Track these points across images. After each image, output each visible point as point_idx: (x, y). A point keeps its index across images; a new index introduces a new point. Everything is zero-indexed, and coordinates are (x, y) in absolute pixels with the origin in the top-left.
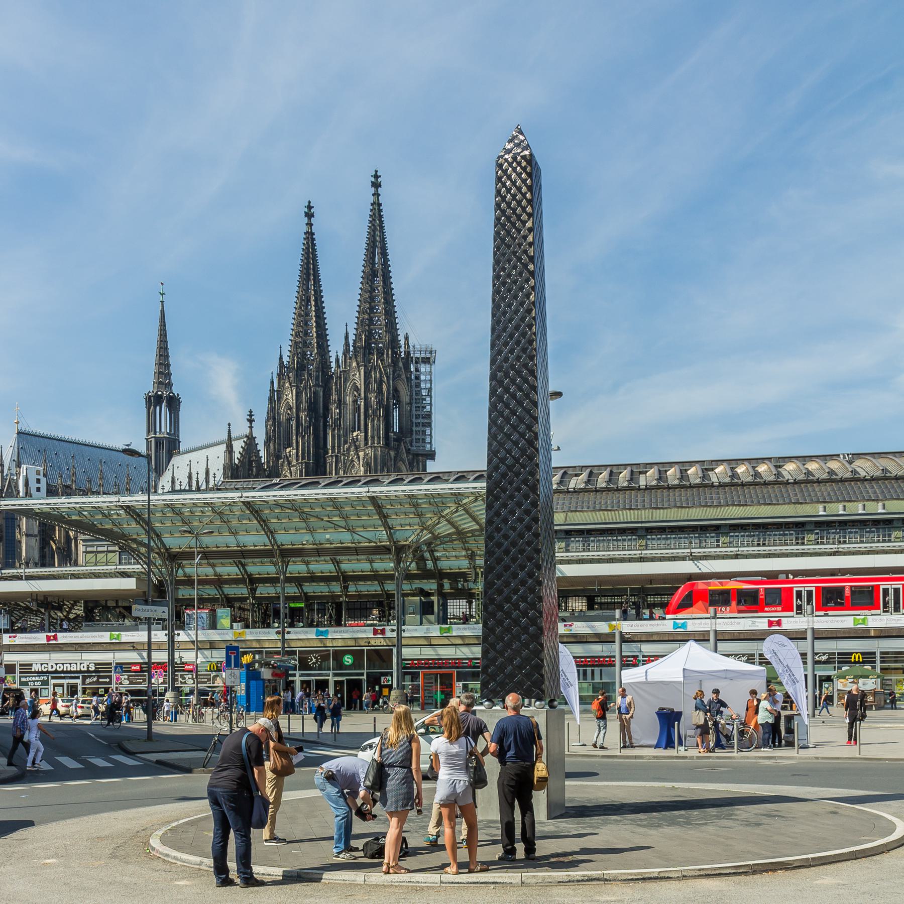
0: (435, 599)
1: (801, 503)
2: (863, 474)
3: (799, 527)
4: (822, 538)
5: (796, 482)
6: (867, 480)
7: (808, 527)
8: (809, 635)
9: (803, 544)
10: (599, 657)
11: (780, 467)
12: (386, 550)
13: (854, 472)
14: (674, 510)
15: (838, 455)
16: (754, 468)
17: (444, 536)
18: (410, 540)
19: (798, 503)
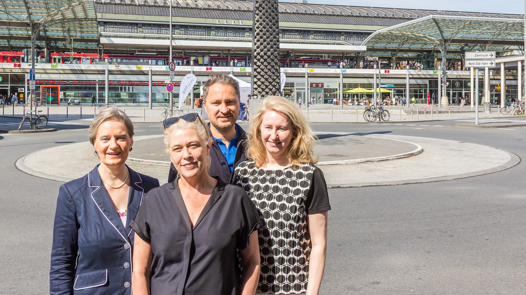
0: (45, 50)
2: (200, 6)
3: (208, 28)
4: (218, 33)
7: (212, 29)
8: (150, 73)
10: (39, 80)
12: (28, 25)
14: (153, 17)
17: (56, 20)
18: (40, 20)
19: (206, 18)
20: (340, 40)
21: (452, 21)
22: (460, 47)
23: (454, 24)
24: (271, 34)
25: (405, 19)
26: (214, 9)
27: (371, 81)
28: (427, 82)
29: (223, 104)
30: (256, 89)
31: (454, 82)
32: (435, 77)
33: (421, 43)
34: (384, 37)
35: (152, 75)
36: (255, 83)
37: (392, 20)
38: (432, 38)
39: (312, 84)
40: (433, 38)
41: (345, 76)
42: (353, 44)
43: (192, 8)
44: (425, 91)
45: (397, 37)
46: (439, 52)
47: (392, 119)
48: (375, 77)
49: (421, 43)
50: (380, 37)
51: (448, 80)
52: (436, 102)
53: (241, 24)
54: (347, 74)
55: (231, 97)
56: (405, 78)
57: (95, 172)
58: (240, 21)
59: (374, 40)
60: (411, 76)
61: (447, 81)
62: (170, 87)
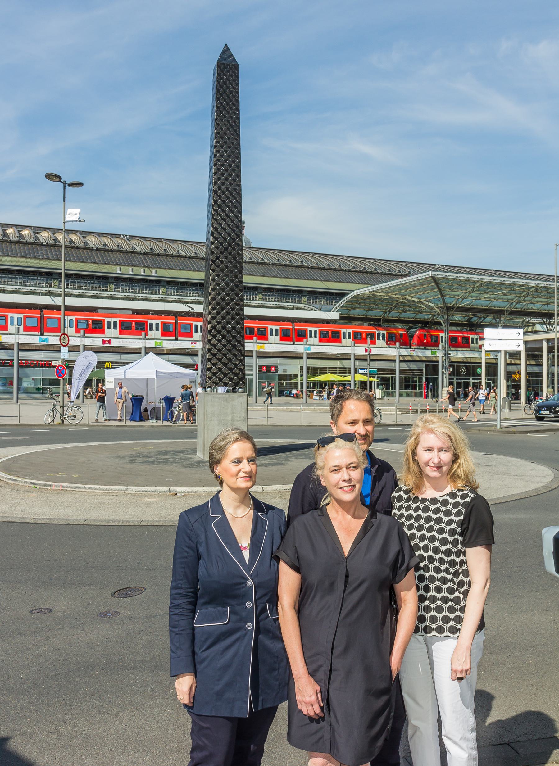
1: (102, 264)
3: (103, 280)
4: (119, 288)
5: (48, 245)
6: (141, 254)
7: (110, 280)
9: (107, 290)
11: (38, 233)
13: (86, 243)
15: (120, 235)
16: (19, 231)
19: (100, 263)
20: (300, 303)
21: (458, 282)
22: (466, 318)
23: (460, 285)
24: (232, 300)
25: (391, 274)
26: (112, 251)
27: (346, 364)
28: (423, 366)
29: (361, 424)
30: (210, 378)
31: (459, 367)
32: (434, 359)
33: (414, 311)
34: (365, 300)
35: (19, 350)
36: (209, 369)
37: (374, 276)
38: (431, 303)
39: (261, 367)
40: (431, 305)
41: (311, 356)
42: (321, 310)
43: (78, 248)
44: (420, 379)
45: (382, 301)
46: (440, 324)
47: (384, 421)
48: (352, 358)
49: (414, 311)
50: (359, 300)
51: (452, 364)
52: (435, 395)
53: (154, 274)
54: (312, 354)
55: (369, 416)
56: (394, 361)
57: (216, 499)
58: (154, 271)
59: (350, 305)
60: (401, 359)
61: (450, 366)
62: (60, 371)
